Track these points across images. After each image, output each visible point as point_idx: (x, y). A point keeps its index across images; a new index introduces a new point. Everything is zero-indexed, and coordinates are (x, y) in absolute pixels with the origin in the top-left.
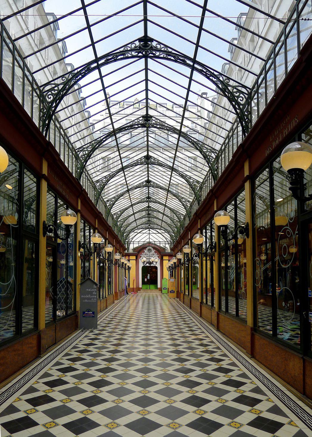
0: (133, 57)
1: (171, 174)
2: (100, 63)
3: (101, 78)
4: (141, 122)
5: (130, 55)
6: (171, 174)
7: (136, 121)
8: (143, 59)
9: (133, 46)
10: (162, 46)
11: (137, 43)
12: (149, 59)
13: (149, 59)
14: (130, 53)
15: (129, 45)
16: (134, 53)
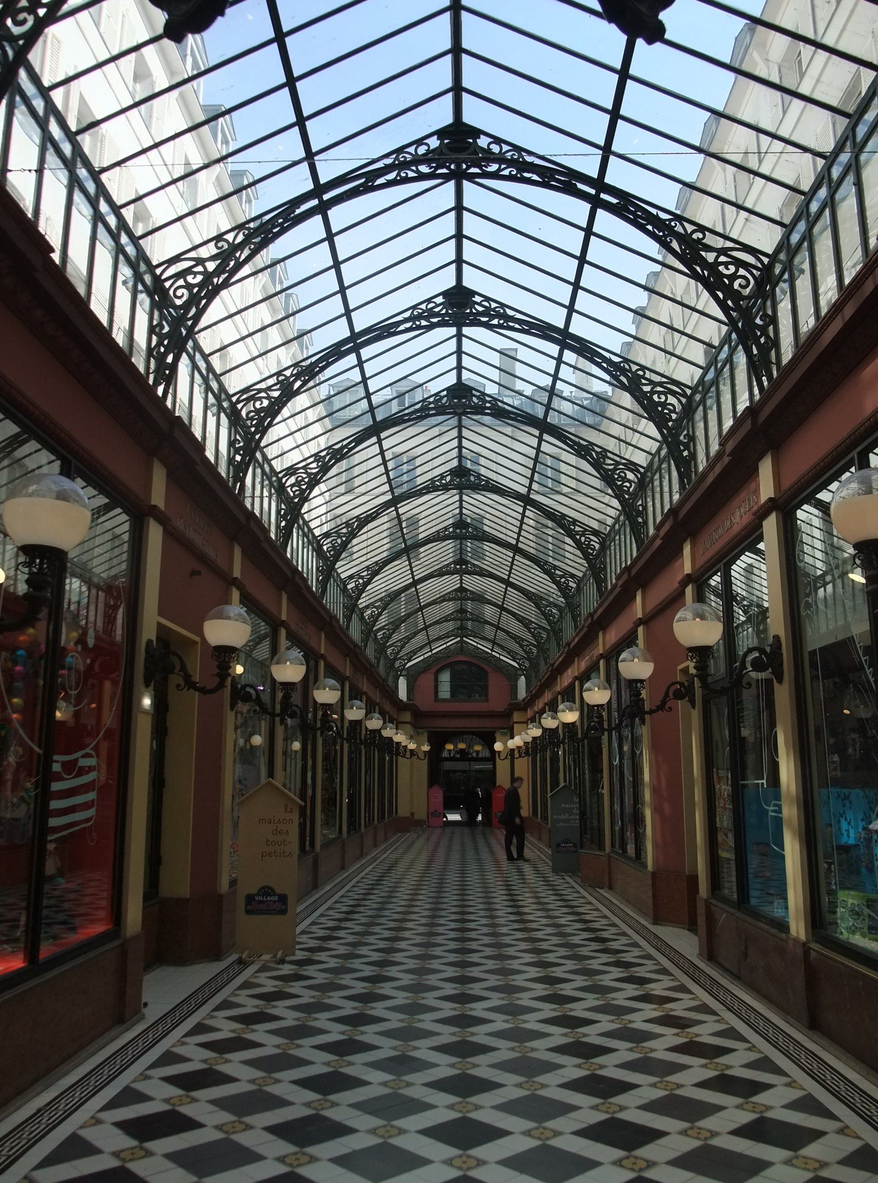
0: (422, 177)
1: (524, 512)
2: (326, 197)
3: (330, 237)
4: (437, 310)
5: (411, 174)
6: (524, 512)
7: (423, 306)
8: (452, 184)
9: (422, 150)
10: (505, 148)
11: (434, 142)
12: (466, 184)
13: (466, 184)
14: (414, 168)
15: (412, 150)
16: (424, 169)
